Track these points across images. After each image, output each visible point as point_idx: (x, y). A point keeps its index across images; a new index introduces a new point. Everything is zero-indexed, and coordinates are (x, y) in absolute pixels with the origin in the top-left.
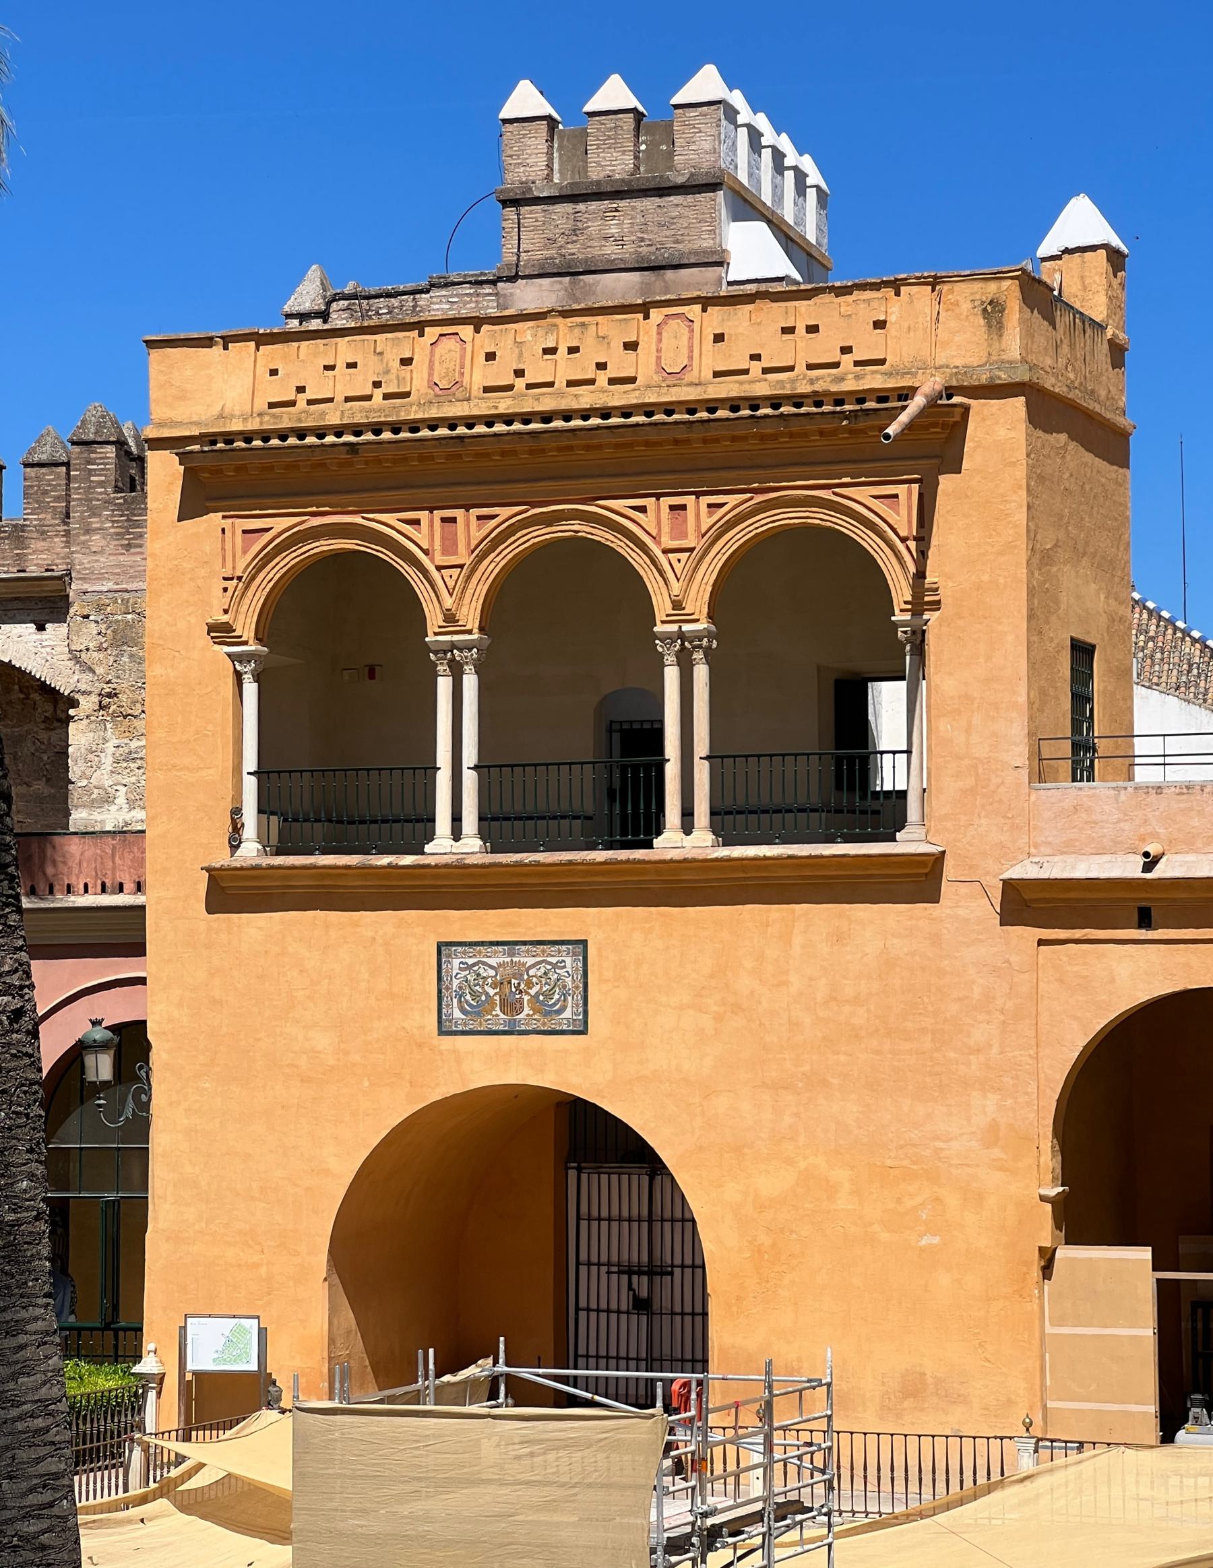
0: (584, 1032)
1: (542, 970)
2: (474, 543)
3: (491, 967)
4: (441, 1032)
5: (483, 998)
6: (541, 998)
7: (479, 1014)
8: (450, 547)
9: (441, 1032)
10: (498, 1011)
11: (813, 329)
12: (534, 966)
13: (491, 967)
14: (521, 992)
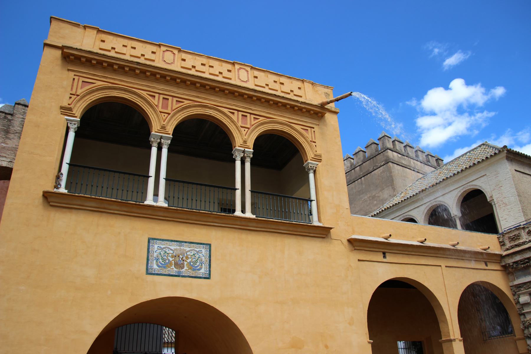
0: (208, 278)
1: (193, 253)
2: (174, 108)
3: (171, 250)
4: (148, 273)
5: (167, 261)
6: (192, 264)
7: (165, 267)
8: (165, 106)
9: (148, 273)
10: (173, 267)
11: (282, 84)
12: (189, 251)
13: (171, 250)
14: (183, 260)
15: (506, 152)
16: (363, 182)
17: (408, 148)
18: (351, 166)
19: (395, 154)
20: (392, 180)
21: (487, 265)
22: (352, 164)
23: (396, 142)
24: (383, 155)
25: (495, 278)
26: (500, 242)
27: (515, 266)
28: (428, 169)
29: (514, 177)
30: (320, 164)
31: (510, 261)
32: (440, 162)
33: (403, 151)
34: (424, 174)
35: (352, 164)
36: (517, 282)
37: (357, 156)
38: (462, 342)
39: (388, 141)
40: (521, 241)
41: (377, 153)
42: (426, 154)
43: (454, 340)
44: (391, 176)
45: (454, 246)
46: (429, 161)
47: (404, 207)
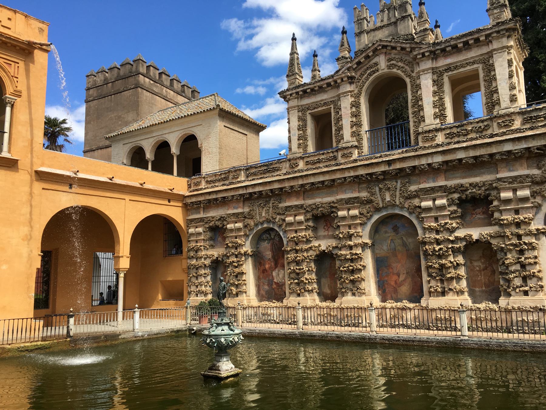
15: (218, 109)
16: (113, 100)
17: (164, 76)
18: (105, 80)
19: (147, 80)
20: (138, 106)
21: (169, 202)
22: (106, 79)
23: (151, 68)
24: (135, 78)
25: (176, 213)
26: (188, 185)
28: (181, 99)
29: (221, 132)
30: (18, 99)
31: (189, 201)
32: (196, 94)
33: (157, 78)
34: (176, 104)
35: (106, 79)
36: (190, 218)
37: (111, 72)
38: (129, 259)
39: (143, 65)
40: (200, 187)
41: (130, 74)
42: (182, 84)
43: (122, 257)
44: (138, 102)
45: (141, 185)
46: (184, 92)
47: (137, 136)
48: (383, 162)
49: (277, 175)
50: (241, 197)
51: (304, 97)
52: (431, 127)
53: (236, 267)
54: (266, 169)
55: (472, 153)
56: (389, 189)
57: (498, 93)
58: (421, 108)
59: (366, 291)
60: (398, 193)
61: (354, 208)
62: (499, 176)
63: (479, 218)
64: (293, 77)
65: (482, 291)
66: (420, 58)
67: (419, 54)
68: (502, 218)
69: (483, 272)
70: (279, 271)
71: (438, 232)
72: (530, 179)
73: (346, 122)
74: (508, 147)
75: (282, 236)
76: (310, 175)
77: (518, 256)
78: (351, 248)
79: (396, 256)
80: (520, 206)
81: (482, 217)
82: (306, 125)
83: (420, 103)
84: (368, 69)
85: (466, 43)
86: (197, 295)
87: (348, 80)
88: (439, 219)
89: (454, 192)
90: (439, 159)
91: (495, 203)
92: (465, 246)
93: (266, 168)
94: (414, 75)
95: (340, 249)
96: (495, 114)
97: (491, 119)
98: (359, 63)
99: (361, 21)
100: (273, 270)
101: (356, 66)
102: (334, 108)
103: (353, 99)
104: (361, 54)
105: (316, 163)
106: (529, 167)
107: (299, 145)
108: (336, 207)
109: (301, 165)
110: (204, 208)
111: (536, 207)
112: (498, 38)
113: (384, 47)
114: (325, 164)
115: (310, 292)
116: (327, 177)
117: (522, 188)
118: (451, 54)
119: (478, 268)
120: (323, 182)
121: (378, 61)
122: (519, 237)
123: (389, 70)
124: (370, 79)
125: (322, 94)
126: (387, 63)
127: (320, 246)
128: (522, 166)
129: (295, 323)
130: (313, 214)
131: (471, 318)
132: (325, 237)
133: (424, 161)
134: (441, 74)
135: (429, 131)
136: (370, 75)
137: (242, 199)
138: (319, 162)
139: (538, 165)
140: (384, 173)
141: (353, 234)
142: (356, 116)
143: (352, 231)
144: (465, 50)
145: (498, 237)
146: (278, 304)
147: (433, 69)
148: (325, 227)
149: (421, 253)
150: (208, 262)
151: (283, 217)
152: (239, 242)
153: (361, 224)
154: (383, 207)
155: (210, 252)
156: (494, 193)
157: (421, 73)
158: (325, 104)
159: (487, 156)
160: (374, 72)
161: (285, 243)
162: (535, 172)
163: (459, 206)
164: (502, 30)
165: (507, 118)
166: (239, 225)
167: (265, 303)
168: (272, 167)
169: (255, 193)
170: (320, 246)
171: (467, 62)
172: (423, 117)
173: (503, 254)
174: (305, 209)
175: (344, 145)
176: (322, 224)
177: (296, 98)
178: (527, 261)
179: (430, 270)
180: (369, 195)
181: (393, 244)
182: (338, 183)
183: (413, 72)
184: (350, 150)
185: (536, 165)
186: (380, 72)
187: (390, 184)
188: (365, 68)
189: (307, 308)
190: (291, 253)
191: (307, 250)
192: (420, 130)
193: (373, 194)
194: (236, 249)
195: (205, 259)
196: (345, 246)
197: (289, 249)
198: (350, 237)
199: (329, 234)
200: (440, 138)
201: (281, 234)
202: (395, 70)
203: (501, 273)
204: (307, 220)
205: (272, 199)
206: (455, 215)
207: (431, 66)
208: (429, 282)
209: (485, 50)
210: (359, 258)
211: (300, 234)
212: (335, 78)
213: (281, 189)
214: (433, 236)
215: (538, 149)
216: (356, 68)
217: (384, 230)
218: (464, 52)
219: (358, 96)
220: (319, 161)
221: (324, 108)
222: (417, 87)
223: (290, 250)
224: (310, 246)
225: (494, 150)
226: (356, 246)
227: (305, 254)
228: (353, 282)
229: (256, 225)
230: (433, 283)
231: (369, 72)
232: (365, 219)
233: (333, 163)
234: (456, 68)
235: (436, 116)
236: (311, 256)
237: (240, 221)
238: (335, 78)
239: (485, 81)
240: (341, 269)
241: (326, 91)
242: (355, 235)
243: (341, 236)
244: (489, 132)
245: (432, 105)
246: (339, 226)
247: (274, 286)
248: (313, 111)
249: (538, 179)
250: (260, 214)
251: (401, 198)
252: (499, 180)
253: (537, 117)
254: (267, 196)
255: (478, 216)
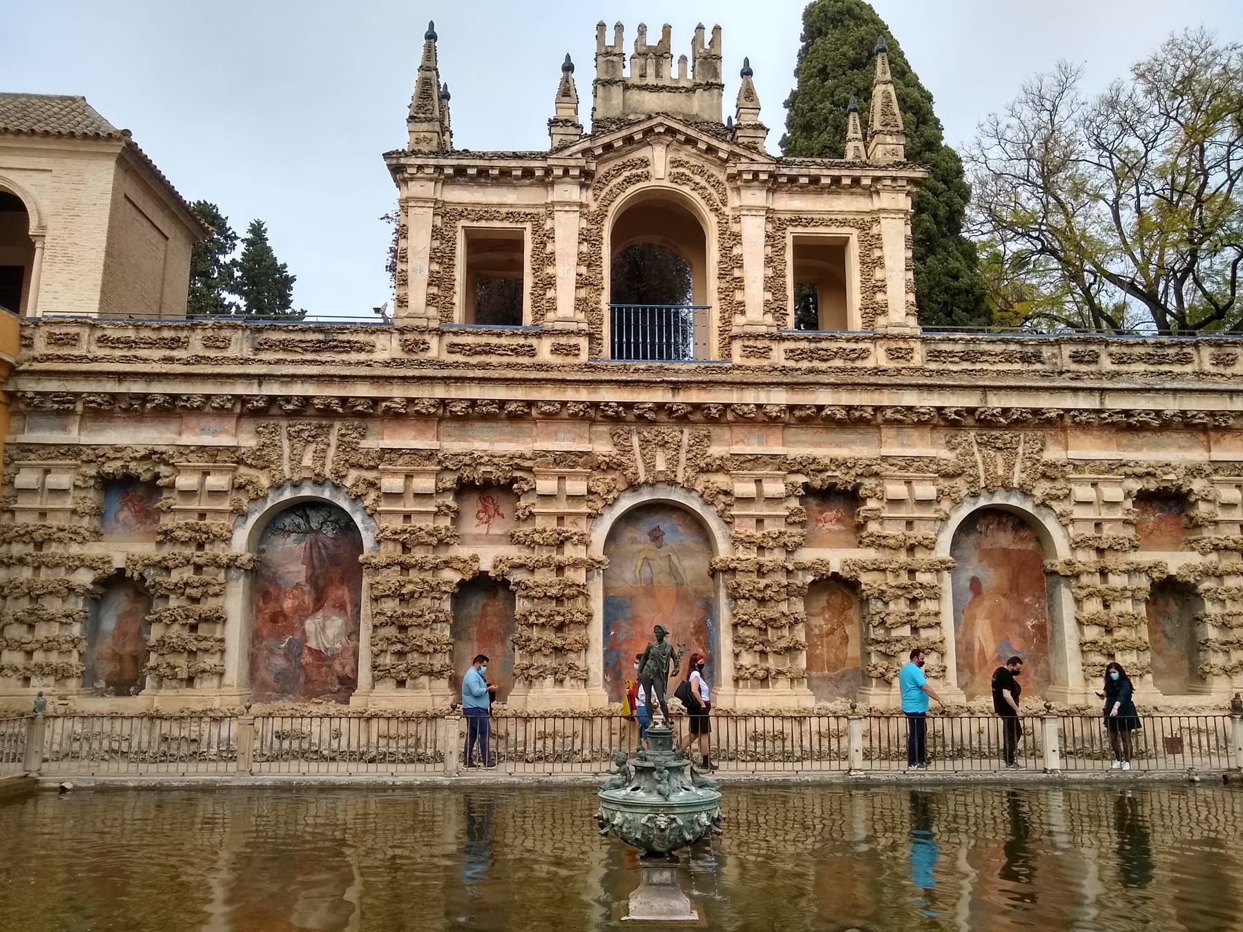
15: (123, 144)
27: (36, 401)
40: (76, 353)
48: (663, 381)
49: (358, 363)
50: (234, 405)
51: (454, 183)
52: (762, 330)
53: (195, 600)
54: (324, 342)
55: (846, 398)
56: (664, 444)
57: (885, 292)
58: (739, 284)
59: (591, 674)
60: (683, 456)
61: (576, 475)
62: (885, 451)
63: (830, 531)
64: (425, 126)
65: (824, 678)
66: (747, 181)
67: (748, 171)
68: (884, 534)
69: (825, 640)
70: (326, 618)
71: (761, 548)
72: (935, 467)
73: (566, 272)
74: (910, 399)
75: (360, 526)
76: (472, 379)
77: (908, 610)
78: (560, 569)
79: (653, 597)
80: (917, 515)
81: (836, 528)
82: (453, 251)
83: (737, 273)
84: (624, 166)
85: (836, 180)
86: (27, 680)
87: (580, 176)
88: (766, 522)
89: (797, 472)
90: (779, 398)
91: (872, 504)
92: (814, 582)
93: (321, 337)
94: (727, 210)
95: (532, 571)
96: (881, 331)
97: (874, 339)
98: (608, 147)
99: (615, 59)
100: (307, 617)
101: (600, 151)
102: (534, 232)
103: (584, 224)
104: (620, 129)
105: (476, 353)
106: (933, 444)
107: (431, 300)
108: (529, 470)
109: (436, 349)
110: (82, 416)
111: (942, 520)
112: (894, 189)
113: (671, 131)
114: (505, 360)
115: (433, 674)
116: (519, 394)
117: (924, 479)
118: (802, 193)
119: (817, 631)
120: (502, 404)
121: (650, 157)
122: (912, 572)
123: (674, 185)
124: (628, 191)
125: (504, 190)
126: (669, 169)
127: (475, 559)
128: (922, 439)
129: (439, 757)
130: (460, 479)
131: (819, 732)
132: (477, 538)
133: (751, 397)
134: (781, 226)
135: (757, 337)
136: (629, 181)
137: (238, 409)
138: (487, 353)
139: (948, 442)
140: (660, 407)
141: (567, 539)
142: (589, 266)
143: (569, 527)
144: (830, 193)
145: (874, 570)
146: (332, 707)
147: (768, 210)
148: (482, 515)
149: (723, 593)
150: (84, 578)
151: (370, 475)
152: (215, 529)
153: (590, 516)
154: (646, 483)
155: (94, 550)
156: (869, 483)
157: (745, 212)
158: (510, 216)
159: (870, 410)
160: (638, 178)
161: (368, 540)
162: (944, 454)
163: (801, 498)
164: (902, 178)
165: (902, 344)
166: (217, 481)
167: (287, 705)
168: (341, 337)
169: (288, 399)
170: (475, 559)
171: (833, 217)
172: (741, 304)
173: (880, 604)
174: (440, 462)
175: (559, 326)
176: (472, 506)
177: (431, 180)
178: (923, 619)
179: (741, 631)
180: (615, 451)
181: (648, 569)
182: (542, 413)
183: (725, 204)
184: (573, 341)
185: (943, 442)
186: (653, 182)
187: (670, 432)
188: (619, 162)
189: (161, 718)
190: (386, 571)
191: (436, 568)
192: (735, 330)
193: (626, 451)
194: (200, 546)
195: (72, 569)
196: (547, 565)
197: (381, 559)
198: (560, 545)
199: (491, 532)
200: (778, 356)
201: (358, 519)
202: (686, 189)
203: (878, 642)
204: (440, 492)
205: (337, 425)
206: (797, 519)
207: (764, 204)
208: (737, 655)
209: (863, 204)
210: (582, 592)
211: (423, 525)
212: (550, 162)
213: (375, 401)
214: (753, 555)
215: (956, 413)
216: (600, 155)
217: (629, 535)
218: (825, 196)
219: (597, 219)
220: (488, 350)
221: (506, 224)
222: (737, 237)
223: (388, 566)
224: (444, 555)
225: (884, 399)
226: (575, 565)
227: (428, 576)
228: (559, 651)
229: (278, 487)
230: (747, 659)
231: (627, 174)
232: (600, 504)
233: (526, 360)
234: (810, 222)
235: (768, 307)
236: (446, 583)
237: (220, 470)
238: (550, 162)
239: (863, 263)
240: (532, 619)
241: (515, 186)
242: (576, 538)
243: (536, 537)
244: (869, 363)
245: (760, 284)
246: (532, 515)
247: (307, 659)
248: (475, 224)
249: (950, 469)
250: (296, 461)
251: (689, 470)
252: (884, 458)
253: (951, 354)
254: (327, 412)
255: (828, 526)
